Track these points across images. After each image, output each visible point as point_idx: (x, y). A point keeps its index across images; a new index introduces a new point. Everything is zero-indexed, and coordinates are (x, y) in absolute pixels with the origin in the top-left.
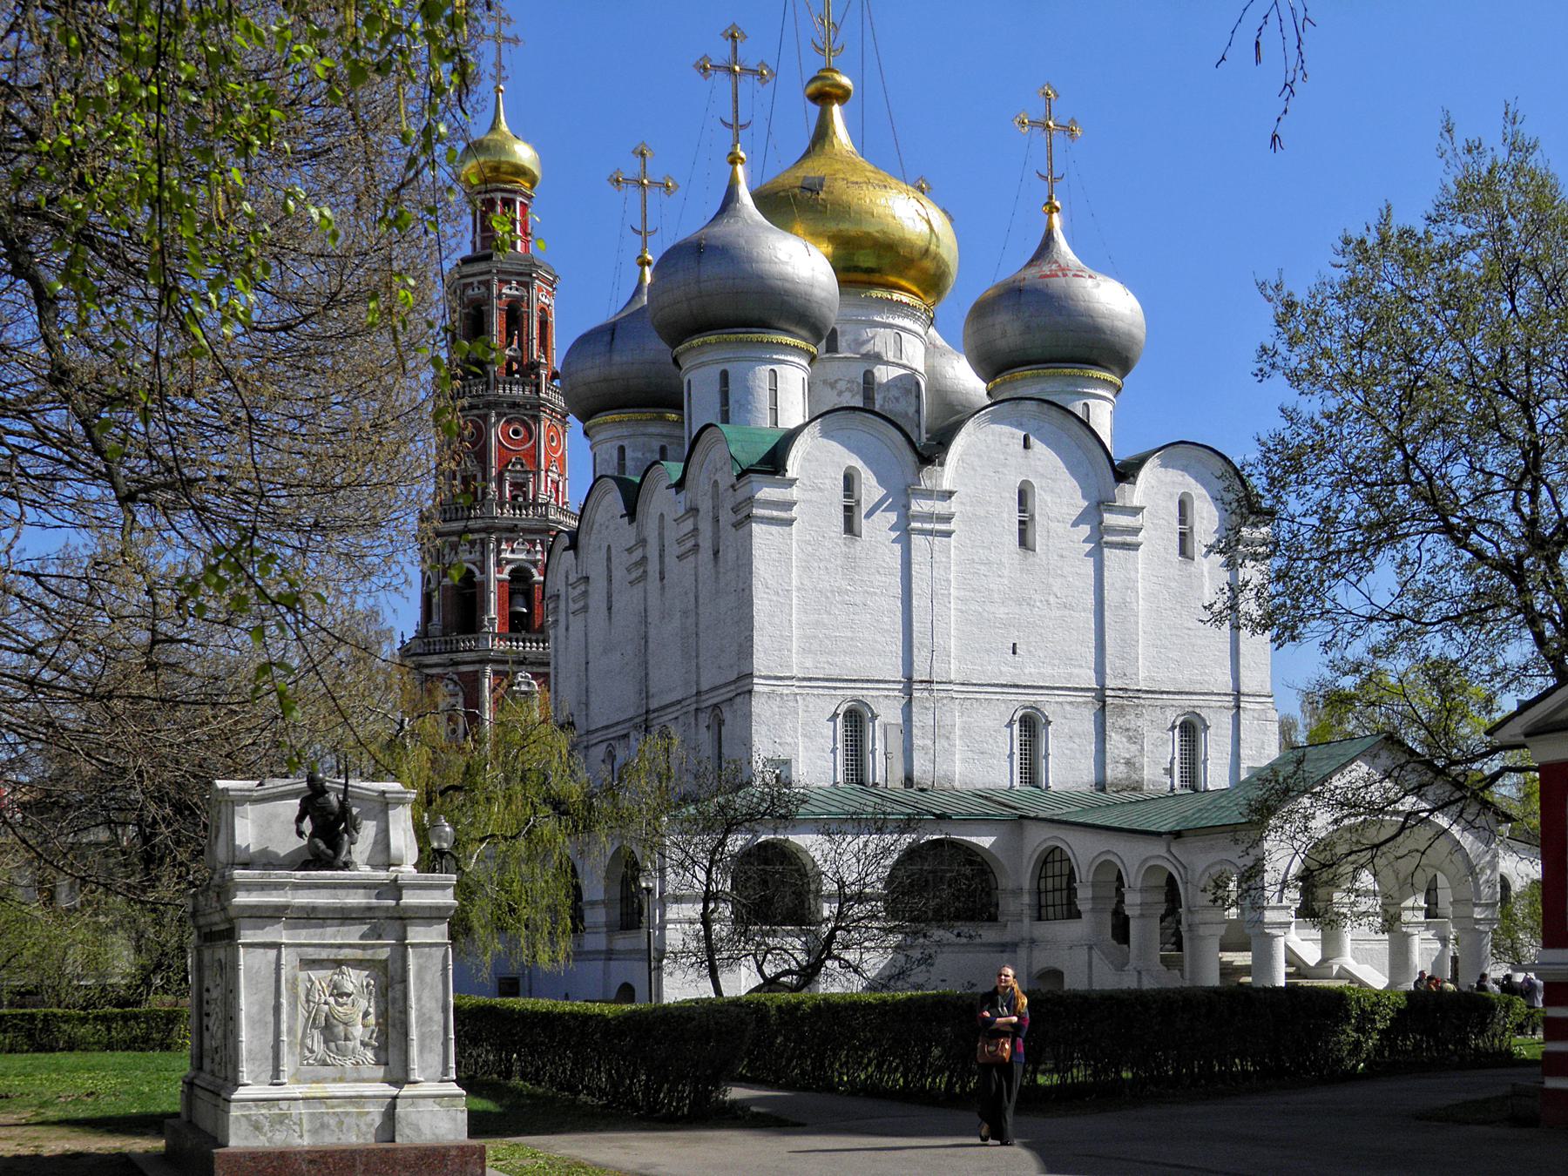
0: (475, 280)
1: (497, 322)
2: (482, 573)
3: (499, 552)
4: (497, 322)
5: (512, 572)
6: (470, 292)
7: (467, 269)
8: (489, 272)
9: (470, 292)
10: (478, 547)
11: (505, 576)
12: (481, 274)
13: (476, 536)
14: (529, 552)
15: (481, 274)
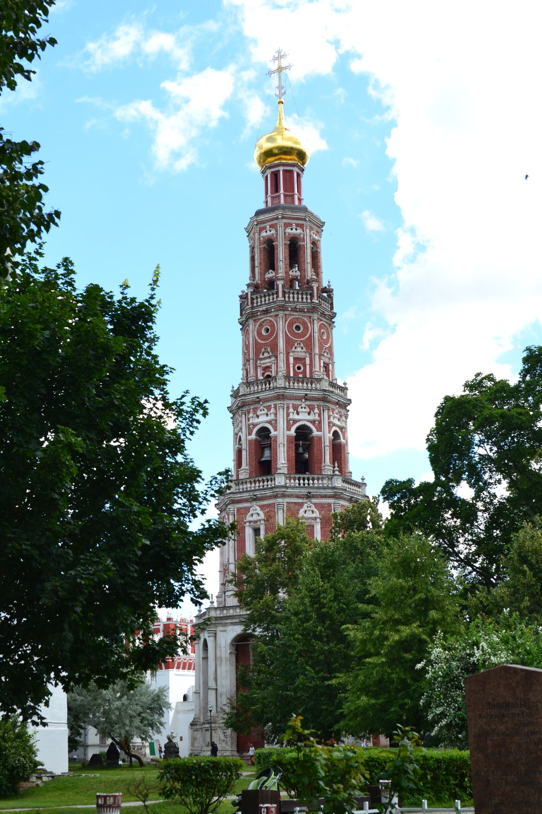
0: (267, 225)
1: (282, 253)
2: (276, 430)
3: (288, 415)
4: (282, 253)
5: (298, 429)
6: (264, 234)
7: (261, 217)
8: (277, 218)
9: (264, 234)
10: (272, 410)
11: (292, 432)
12: (273, 219)
13: (272, 404)
14: (309, 414)
15: (273, 219)
